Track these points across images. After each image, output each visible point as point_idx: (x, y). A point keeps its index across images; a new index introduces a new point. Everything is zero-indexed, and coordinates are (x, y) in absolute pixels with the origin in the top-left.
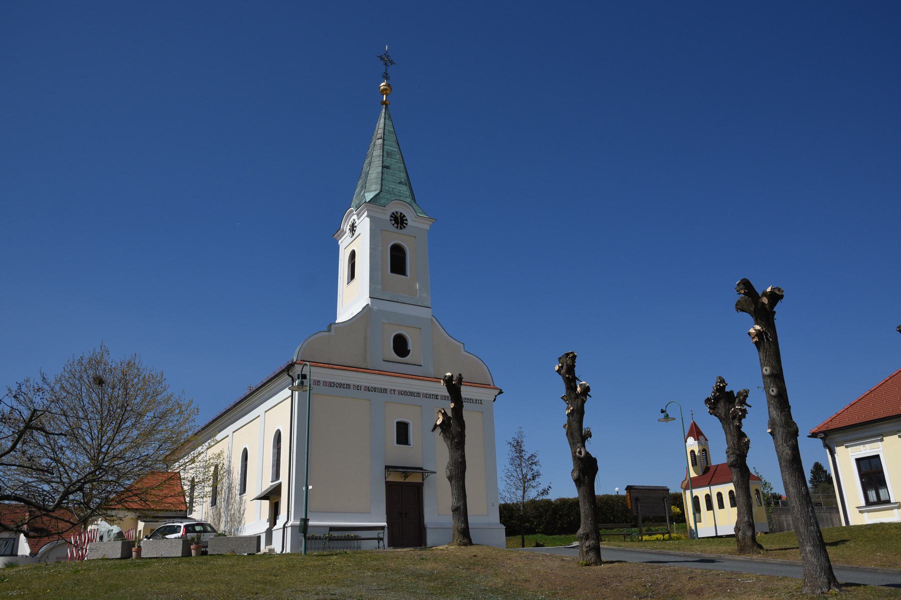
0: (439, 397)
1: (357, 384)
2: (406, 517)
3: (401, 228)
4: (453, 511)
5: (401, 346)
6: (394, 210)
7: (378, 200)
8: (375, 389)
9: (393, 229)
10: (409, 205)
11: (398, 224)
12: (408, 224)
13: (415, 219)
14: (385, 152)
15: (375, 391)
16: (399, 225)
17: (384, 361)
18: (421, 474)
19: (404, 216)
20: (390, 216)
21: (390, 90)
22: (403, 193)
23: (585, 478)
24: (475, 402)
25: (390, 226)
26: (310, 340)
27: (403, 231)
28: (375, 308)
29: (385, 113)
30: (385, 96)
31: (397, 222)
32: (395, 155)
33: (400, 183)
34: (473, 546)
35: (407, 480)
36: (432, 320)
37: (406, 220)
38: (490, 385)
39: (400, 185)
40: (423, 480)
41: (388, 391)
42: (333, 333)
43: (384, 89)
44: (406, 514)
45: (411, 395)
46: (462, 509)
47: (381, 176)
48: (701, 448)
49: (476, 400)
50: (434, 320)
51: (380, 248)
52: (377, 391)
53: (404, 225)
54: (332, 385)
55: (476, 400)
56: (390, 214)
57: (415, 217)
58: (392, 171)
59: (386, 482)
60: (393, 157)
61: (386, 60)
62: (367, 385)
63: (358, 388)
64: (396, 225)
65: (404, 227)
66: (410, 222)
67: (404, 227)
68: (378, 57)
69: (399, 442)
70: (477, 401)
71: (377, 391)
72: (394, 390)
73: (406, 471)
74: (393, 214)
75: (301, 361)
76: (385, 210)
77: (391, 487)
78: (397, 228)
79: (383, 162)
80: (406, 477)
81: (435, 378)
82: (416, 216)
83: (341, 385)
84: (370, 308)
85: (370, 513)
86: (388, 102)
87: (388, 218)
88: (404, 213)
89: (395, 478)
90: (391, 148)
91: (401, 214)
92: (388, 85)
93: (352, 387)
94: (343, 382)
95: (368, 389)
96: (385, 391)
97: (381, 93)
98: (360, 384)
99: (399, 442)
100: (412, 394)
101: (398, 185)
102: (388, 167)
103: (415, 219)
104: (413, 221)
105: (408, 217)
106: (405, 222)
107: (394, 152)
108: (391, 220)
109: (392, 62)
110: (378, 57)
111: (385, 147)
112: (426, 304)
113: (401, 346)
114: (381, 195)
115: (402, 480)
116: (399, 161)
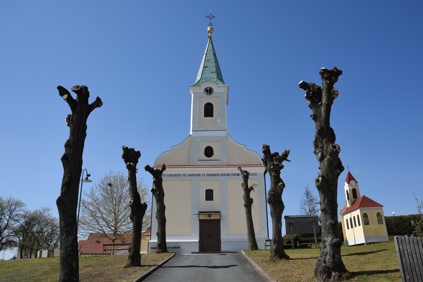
0: (230, 175)
1: (184, 173)
2: (211, 236)
3: (210, 94)
4: (157, 235)
5: (209, 152)
6: (206, 87)
7: (199, 84)
8: (194, 175)
9: (206, 96)
10: (213, 83)
11: (208, 93)
13: (218, 88)
14: (206, 60)
15: (194, 176)
16: (209, 93)
17: (199, 160)
18: (220, 215)
19: (212, 88)
20: (214, 90)
21: (212, 31)
22: (213, 77)
23: (134, 216)
24: (252, 175)
25: (205, 95)
26: (160, 156)
27: (211, 96)
28: (195, 136)
29: (209, 42)
30: (210, 34)
32: (211, 60)
33: (212, 73)
34: (168, 253)
35: (211, 218)
36: (226, 136)
37: (213, 90)
38: (262, 165)
39: (212, 74)
40: (220, 218)
41: (201, 175)
42: (172, 151)
43: (209, 31)
44: (211, 235)
45: (214, 176)
48: (351, 188)
49: (253, 174)
50: (228, 136)
51: (198, 106)
52: (195, 175)
53: (212, 92)
54: (171, 175)
55: (253, 174)
56: (204, 88)
57: (217, 87)
58: (208, 68)
59: (199, 220)
61: (211, 17)
62: (189, 173)
63: (185, 175)
64: (207, 94)
65: (212, 93)
66: (215, 91)
67: (212, 93)
68: (215, 17)
69: (207, 199)
70: (254, 174)
71: (195, 175)
72: (204, 174)
73: (209, 213)
74: (206, 88)
75: (156, 166)
76: (200, 88)
77: (202, 222)
78: (208, 95)
79: (204, 65)
80: (210, 216)
81: (228, 165)
82: (218, 87)
83: (176, 175)
84: (192, 136)
86: (211, 37)
87: (203, 91)
88: (211, 87)
89: (203, 217)
90: (210, 57)
91: (210, 87)
92: (211, 28)
93: (220, 175)
94: (176, 173)
95: (190, 175)
96: (199, 175)
97: (209, 32)
99: (207, 199)
100: (214, 175)
101: (211, 74)
102: (206, 67)
103: (218, 88)
105: (213, 88)
106: (212, 91)
108: (204, 92)
109: (213, 17)
110: (206, 17)
111: (206, 57)
112: (224, 129)
113: (209, 152)
114: (200, 81)
115: (208, 218)
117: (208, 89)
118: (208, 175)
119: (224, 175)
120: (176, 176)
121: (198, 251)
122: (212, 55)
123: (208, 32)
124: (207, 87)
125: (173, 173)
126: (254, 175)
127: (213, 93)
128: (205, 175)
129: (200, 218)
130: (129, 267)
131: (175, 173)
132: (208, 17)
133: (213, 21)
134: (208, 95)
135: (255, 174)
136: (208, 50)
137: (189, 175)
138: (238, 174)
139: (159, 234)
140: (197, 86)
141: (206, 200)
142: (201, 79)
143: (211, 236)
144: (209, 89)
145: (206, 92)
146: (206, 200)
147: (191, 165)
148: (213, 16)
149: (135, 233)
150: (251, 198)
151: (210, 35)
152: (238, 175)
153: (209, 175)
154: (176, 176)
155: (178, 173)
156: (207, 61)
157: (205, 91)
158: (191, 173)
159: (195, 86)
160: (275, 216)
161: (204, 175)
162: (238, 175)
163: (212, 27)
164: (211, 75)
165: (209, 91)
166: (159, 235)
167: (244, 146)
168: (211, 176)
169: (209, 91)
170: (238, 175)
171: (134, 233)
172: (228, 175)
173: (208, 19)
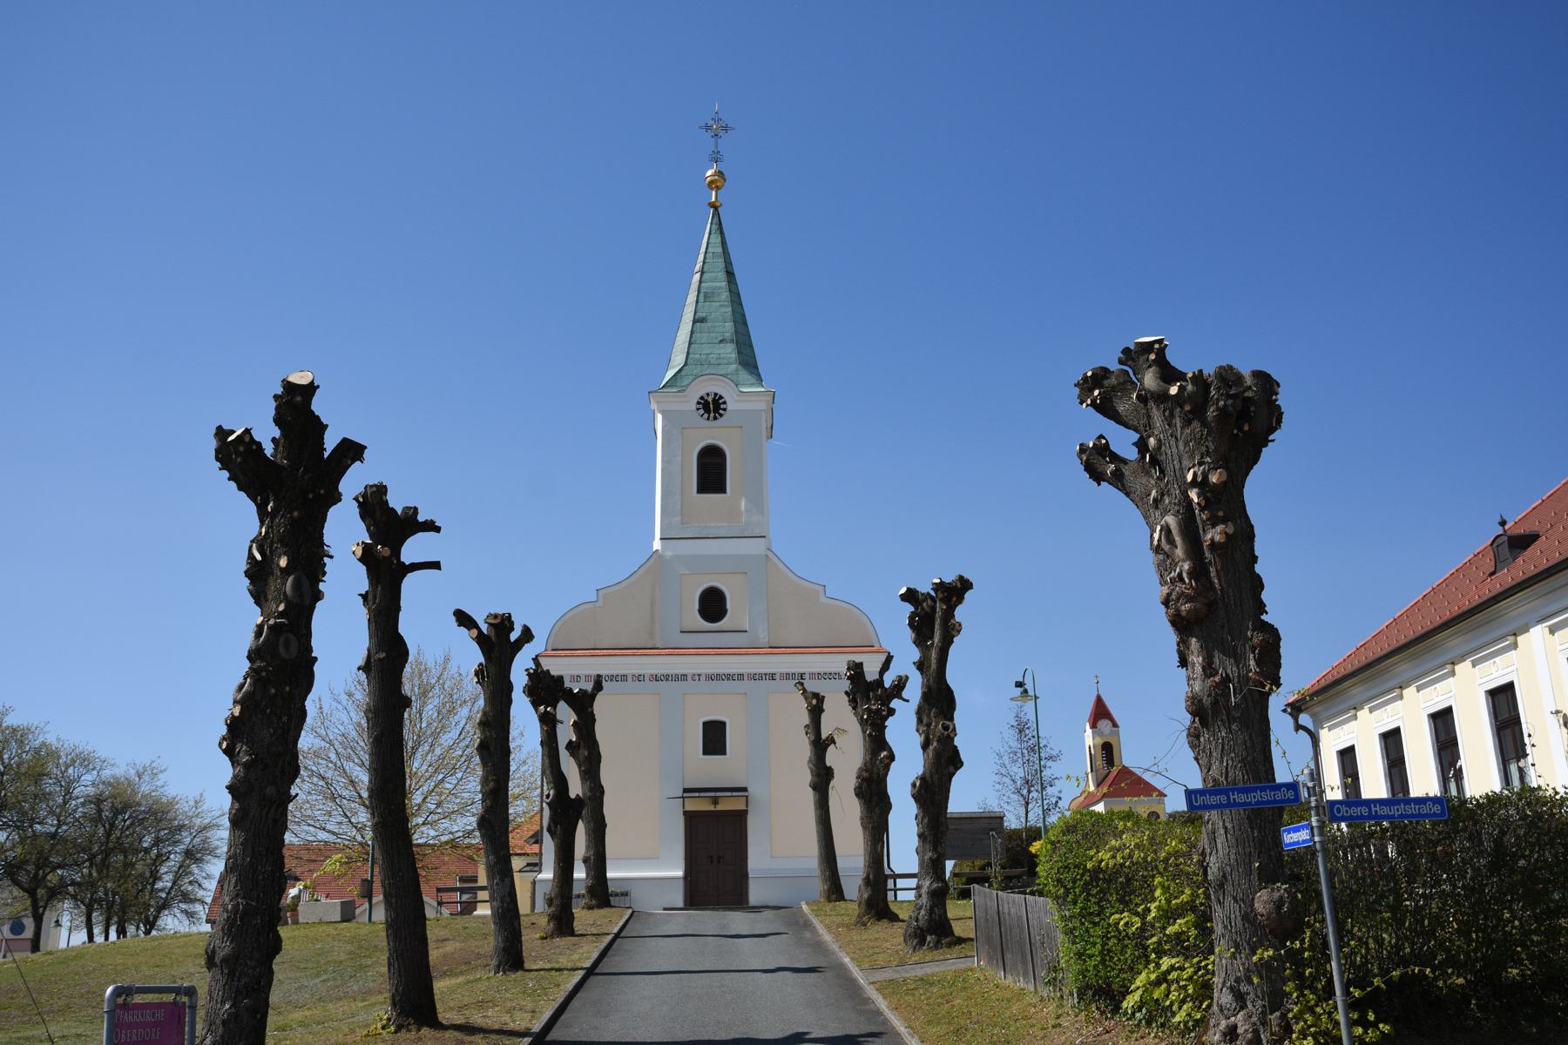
0: (777, 677)
1: (637, 672)
2: (719, 862)
3: (715, 418)
5: (713, 605)
6: (702, 392)
7: (678, 380)
8: (667, 677)
12: (729, 408)
15: (667, 680)
17: (682, 632)
19: (721, 397)
20: (723, 395)
21: (722, 181)
22: (724, 358)
25: (697, 418)
26: (563, 619)
27: (720, 421)
28: (669, 554)
29: (711, 224)
30: (714, 193)
31: (707, 410)
32: (719, 294)
33: (721, 341)
35: (719, 808)
36: (767, 556)
37: (725, 403)
38: (873, 646)
39: (721, 345)
40: (747, 806)
41: (689, 678)
42: (600, 603)
43: (712, 182)
45: (728, 679)
46: (592, 861)
47: (688, 339)
48: (1100, 741)
50: (769, 553)
51: (679, 458)
52: (670, 679)
53: (721, 411)
56: (696, 398)
57: (739, 396)
59: (685, 813)
60: (716, 299)
61: (718, 129)
62: (654, 672)
63: (639, 678)
64: (706, 415)
65: (721, 415)
66: (731, 406)
67: (721, 415)
69: (706, 752)
71: (670, 679)
72: (699, 675)
73: (714, 792)
74: (702, 398)
75: (552, 650)
76: (686, 396)
77: (691, 818)
79: (695, 312)
81: (770, 648)
84: (660, 556)
85: (658, 858)
86: (718, 204)
87: (693, 406)
88: (720, 392)
89: (694, 805)
90: (715, 284)
91: (716, 394)
92: (720, 173)
94: (615, 672)
95: (656, 678)
96: (684, 677)
98: (641, 672)
99: (706, 752)
100: (729, 677)
101: (717, 346)
102: (702, 320)
104: (736, 401)
105: (727, 397)
106: (722, 406)
107: (720, 288)
108: (698, 409)
109: (726, 129)
111: (702, 284)
112: (757, 532)
113: (713, 605)
114: (683, 373)
115: (711, 808)
116: (726, 303)
117: (710, 399)
118: (710, 677)
121: (681, 904)
122: (722, 275)
127: (726, 416)
128: (703, 678)
129: (687, 809)
132: (708, 128)
134: (708, 419)
142: (686, 364)
143: (719, 862)
144: (714, 400)
145: (702, 411)
150: (828, 765)
151: (713, 199)
156: (706, 296)
157: (701, 406)
160: (871, 826)
164: (719, 351)
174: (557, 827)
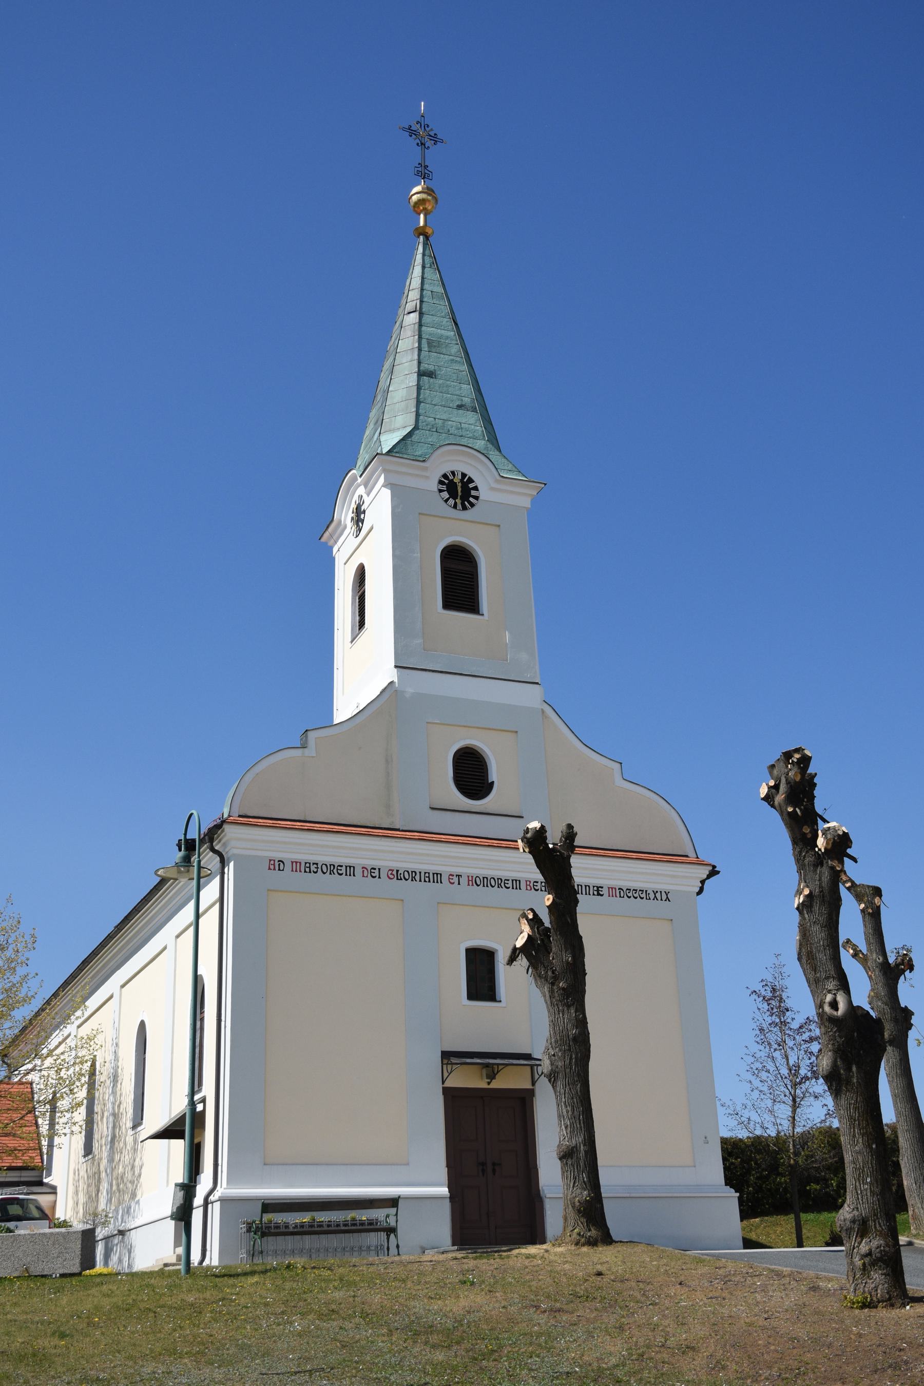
1: (370, 863)
2: (494, 1171)
4: (560, 1159)
6: (446, 468)
7: (410, 447)
8: (413, 875)
9: (446, 510)
11: (455, 498)
12: (481, 498)
13: (498, 486)
14: (424, 342)
15: (413, 879)
16: (459, 501)
17: (433, 809)
18: (528, 1068)
19: (471, 480)
21: (433, 202)
24: (652, 896)
25: (439, 504)
26: (257, 769)
27: (469, 514)
28: (410, 690)
29: (424, 255)
30: (422, 216)
31: (453, 494)
33: (460, 407)
34: (611, 1248)
35: (496, 1084)
36: (543, 711)
37: (476, 488)
38: (687, 856)
39: (461, 412)
40: (533, 1083)
41: (445, 879)
42: (311, 751)
43: (421, 202)
44: (494, 1164)
45: (499, 886)
46: (582, 1154)
47: (415, 395)
49: (655, 893)
52: (417, 877)
53: (471, 499)
54: (313, 868)
55: (655, 893)
56: (437, 476)
57: (496, 481)
58: (441, 382)
60: (444, 351)
62: (395, 865)
63: (373, 872)
64: (451, 502)
65: (472, 505)
66: (483, 493)
67: (472, 505)
69: (473, 995)
70: (658, 895)
71: (417, 877)
72: (459, 876)
74: (445, 476)
75: (240, 816)
76: (426, 469)
78: (455, 506)
79: (419, 363)
80: (492, 1077)
82: (498, 478)
83: (333, 869)
85: (408, 1164)
86: (429, 231)
87: (434, 486)
88: (470, 473)
91: (464, 475)
92: (429, 191)
94: (336, 860)
95: (397, 875)
96: (437, 877)
97: (415, 211)
98: (376, 863)
99: (473, 995)
101: (455, 411)
102: (431, 374)
103: (498, 486)
104: (492, 489)
105: (478, 481)
106: (473, 493)
107: (447, 338)
108: (440, 491)
109: (435, 139)
111: (424, 328)
114: (415, 438)
115: (482, 1084)
116: (458, 359)
117: (457, 480)
118: (475, 881)
119: (539, 887)
120: (335, 871)
122: (447, 322)
123: (414, 207)
124: (452, 469)
125: (321, 859)
126: (659, 899)
127: (479, 505)
128: (464, 880)
129: (447, 1084)
130: (892, 1305)
131: (329, 860)
132: (411, 132)
133: (434, 156)
134: (455, 506)
135: (664, 897)
136: (425, 292)
137: (395, 873)
138: (598, 887)
139: (578, 1151)
140: (405, 456)
141: (471, 997)
142: (416, 428)
143: (494, 1171)
144: (462, 480)
145: (446, 495)
146: (471, 997)
147: (397, 827)
148: (432, 133)
149: (874, 1146)
150: (903, 1005)
151: (422, 223)
152: (598, 891)
153: (478, 883)
154: (335, 871)
155: (433, 868)
156: (430, 343)
157: (444, 488)
158: (403, 866)
159: (398, 455)
161: (456, 879)
162: (599, 894)
163: (431, 184)
164: (459, 419)
165: (460, 494)
166: (578, 1159)
167: (619, 765)
168: (515, 890)
169: (460, 494)
170: (598, 891)
171: (870, 1146)
172: (596, 893)
173: (413, 141)
174: (849, 1069)
